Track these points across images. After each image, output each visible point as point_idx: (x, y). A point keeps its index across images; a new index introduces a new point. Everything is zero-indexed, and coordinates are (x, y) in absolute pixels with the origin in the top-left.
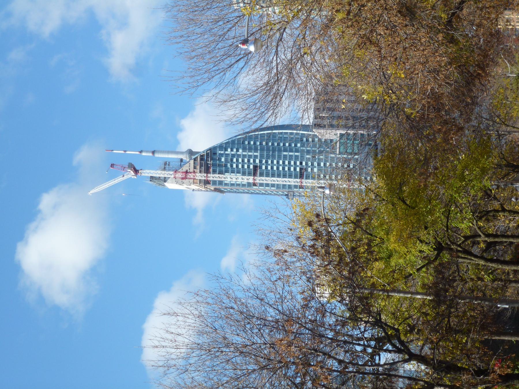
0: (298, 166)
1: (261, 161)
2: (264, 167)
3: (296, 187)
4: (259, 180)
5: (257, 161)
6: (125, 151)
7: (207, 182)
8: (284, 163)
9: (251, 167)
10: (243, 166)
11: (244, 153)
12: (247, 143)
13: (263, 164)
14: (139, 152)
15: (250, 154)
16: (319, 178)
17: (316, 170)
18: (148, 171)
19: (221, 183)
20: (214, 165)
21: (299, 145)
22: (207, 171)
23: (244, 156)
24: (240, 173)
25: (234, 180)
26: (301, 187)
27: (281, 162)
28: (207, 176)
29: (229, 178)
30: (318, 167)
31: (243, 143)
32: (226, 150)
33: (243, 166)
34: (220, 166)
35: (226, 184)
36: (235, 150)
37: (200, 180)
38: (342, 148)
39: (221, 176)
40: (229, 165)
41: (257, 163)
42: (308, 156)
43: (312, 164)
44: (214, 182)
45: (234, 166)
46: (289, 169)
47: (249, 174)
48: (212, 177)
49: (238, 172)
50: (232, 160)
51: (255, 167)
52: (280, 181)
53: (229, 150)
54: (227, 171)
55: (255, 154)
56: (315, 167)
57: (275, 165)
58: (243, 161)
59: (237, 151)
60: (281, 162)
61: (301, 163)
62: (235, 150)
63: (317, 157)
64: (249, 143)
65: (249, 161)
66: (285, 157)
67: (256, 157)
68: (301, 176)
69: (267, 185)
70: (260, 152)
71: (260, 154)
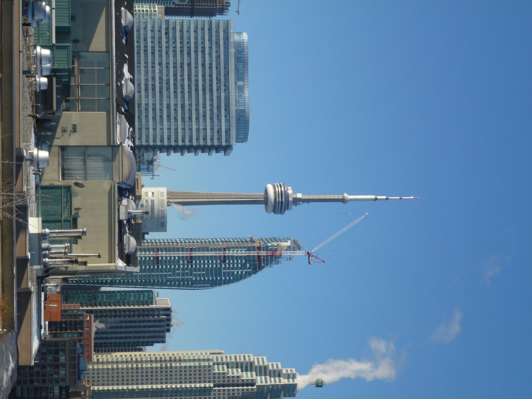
0: (194, 264)
1: (221, 266)
2: (219, 261)
3: (195, 250)
4: (221, 254)
5: (223, 266)
6: (401, 199)
7: (259, 248)
8: (204, 266)
9: (227, 261)
10: (233, 261)
11: (233, 271)
12: (232, 278)
13: (219, 264)
14: (389, 199)
15: (229, 271)
16: (179, 257)
17: (181, 262)
18: (300, 254)
19: (249, 249)
20: (254, 261)
21: (194, 279)
22: (259, 257)
23: (233, 268)
24: (235, 256)
25: (239, 252)
26: (191, 250)
27: (206, 266)
28: (258, 254)
29: (243, 253)
30: (180, 264)
31: (234, 278)
32: (246, 272)
33: (233, 261)
34: (250, 261)
35: (245, 248)
36: (240, 273)
37: (264, 251)
38: (151, 296)
39: (248, 254)
40: (244, 261)
41: (223, 264)
42: (187, 271)
43: (184, 266)
44: (254, 249)
45: (239, 261)
46: (200, 262)
47: (229, 256)
48: (254, 253)
49: (237, 257)
50: (241, 265)
51: (225, 261)
52: (206, 254)
53: (244, 273)
54: (245, 257)
55: (225, 271)
56: (182, 264)
57: (210, 264)
58: (233, 265)
59: (238, 272)
60: (206, 266)
61: (192, 266)
62: (240, 273)
63: (181, 271)
64: (230, 278)
65: (229, 265)
66: (203, 270)
67: (224, 268)
68: (191, 257)
69: (215, 250)
70: (221, 272)
71: (221, 271)
